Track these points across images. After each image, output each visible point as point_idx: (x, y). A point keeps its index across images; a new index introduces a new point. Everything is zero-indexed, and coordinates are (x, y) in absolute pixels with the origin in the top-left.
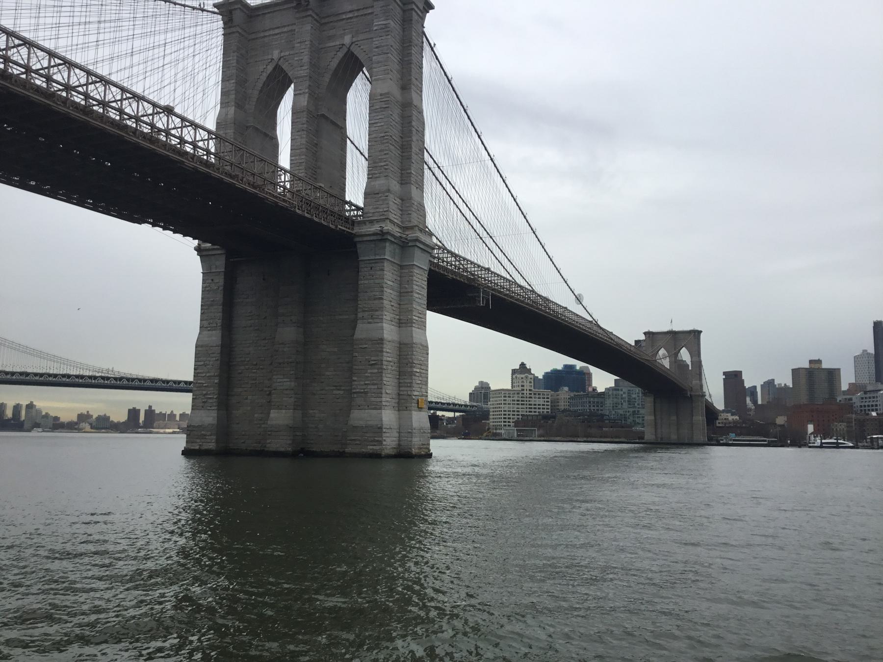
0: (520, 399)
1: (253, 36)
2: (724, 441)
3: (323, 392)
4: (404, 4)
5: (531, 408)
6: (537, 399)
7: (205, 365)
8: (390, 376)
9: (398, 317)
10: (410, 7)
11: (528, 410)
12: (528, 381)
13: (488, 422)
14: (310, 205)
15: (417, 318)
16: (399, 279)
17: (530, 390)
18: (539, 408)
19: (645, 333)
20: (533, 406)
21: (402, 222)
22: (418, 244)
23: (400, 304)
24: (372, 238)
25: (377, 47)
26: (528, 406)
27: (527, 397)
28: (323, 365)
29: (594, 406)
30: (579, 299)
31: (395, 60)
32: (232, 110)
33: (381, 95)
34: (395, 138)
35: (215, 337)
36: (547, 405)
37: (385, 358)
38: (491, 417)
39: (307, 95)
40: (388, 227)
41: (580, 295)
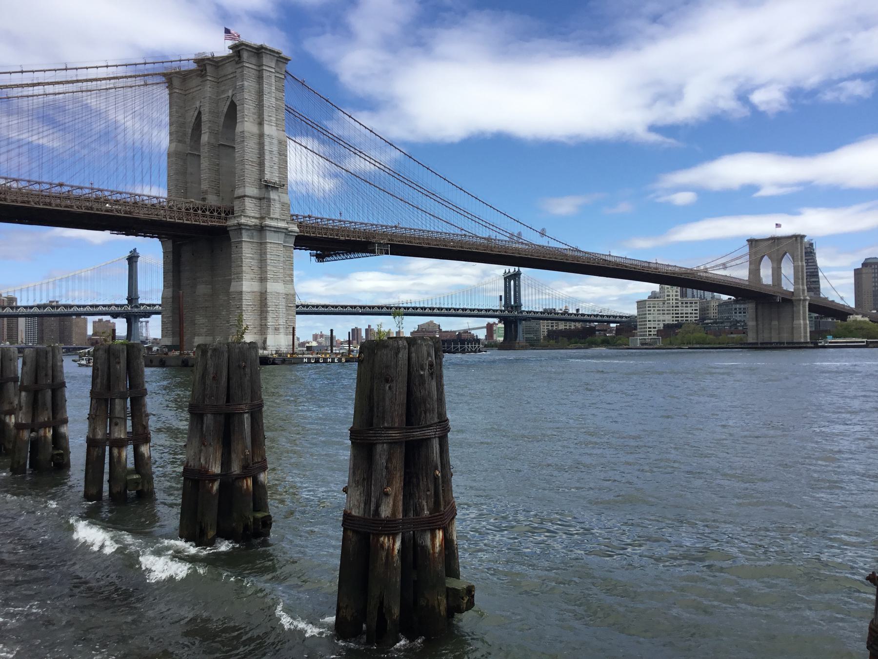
0: (666, 309)
1: (187, 92)
2: (823, 344)
3: (222, 325)
4: (259, 66)
5: (678, 317)
6: (684, 308)
7: (166, 310)
8: (251, 314)
9: (259, 276)
10: (261, 68)
11: (675, 319)
12: (674, 291)
13: (635, 331)
14: (182, 215)
15: (272, 276)
16: (259, 251)
17: (676, 299)
18: (686, 317)
19: (748, 240)
20: (680, 315)
21: (261, 214)
22: (268, 229)
23: (261, 268)
24: (236, 228)
25: (239, 100)
26: (675, 315)
27: (673, 307)
28: (221, 308)
29: (740, 313)
30: (543, 234)
31: (251, 107)
32: (174, 144)
33: (241, 132)
34: (252, 160)
35: (170, 294)
36: (695, 314)
37: (244, 303)
38: (638, 327)
39: (208, 133)
40: (243, 220)
41: (543, 230)
